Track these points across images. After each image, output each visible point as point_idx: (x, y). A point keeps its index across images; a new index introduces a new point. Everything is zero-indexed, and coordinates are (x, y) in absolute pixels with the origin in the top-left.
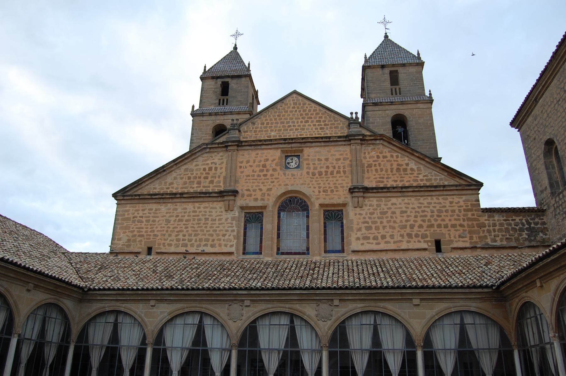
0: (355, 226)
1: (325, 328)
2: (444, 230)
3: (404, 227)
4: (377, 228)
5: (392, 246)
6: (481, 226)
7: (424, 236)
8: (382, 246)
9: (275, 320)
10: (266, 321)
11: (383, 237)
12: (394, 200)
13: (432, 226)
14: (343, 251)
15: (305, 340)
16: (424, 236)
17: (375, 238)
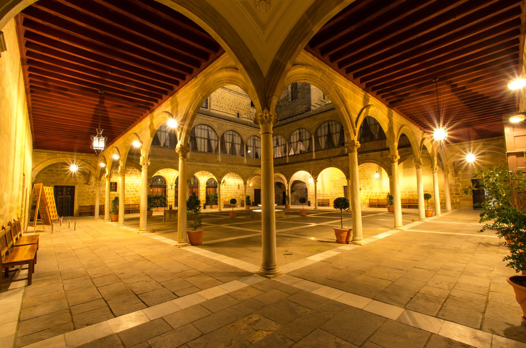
0: (213, 100)
1: (220, 133)
2: (240, 111)
3: (229, 105)
4: (220, 103)
5: (224, 111)
6: (250, 112)
7: (235, 111)
8: (222, 110)
9: (203, 127)
10: (199, 126)
11: (222, 107)
12: (226, 94)
13: (237, 108)
14: (207, 108)
15: (213, 136)
16: (235, 111)
17: (220, 107)
